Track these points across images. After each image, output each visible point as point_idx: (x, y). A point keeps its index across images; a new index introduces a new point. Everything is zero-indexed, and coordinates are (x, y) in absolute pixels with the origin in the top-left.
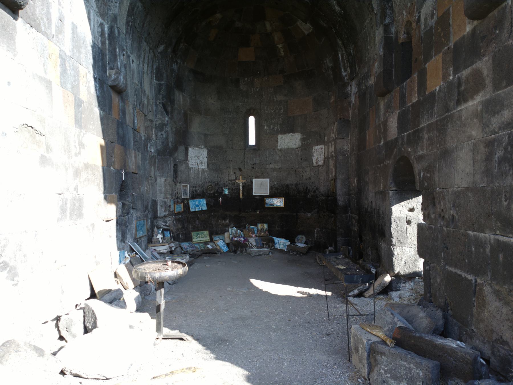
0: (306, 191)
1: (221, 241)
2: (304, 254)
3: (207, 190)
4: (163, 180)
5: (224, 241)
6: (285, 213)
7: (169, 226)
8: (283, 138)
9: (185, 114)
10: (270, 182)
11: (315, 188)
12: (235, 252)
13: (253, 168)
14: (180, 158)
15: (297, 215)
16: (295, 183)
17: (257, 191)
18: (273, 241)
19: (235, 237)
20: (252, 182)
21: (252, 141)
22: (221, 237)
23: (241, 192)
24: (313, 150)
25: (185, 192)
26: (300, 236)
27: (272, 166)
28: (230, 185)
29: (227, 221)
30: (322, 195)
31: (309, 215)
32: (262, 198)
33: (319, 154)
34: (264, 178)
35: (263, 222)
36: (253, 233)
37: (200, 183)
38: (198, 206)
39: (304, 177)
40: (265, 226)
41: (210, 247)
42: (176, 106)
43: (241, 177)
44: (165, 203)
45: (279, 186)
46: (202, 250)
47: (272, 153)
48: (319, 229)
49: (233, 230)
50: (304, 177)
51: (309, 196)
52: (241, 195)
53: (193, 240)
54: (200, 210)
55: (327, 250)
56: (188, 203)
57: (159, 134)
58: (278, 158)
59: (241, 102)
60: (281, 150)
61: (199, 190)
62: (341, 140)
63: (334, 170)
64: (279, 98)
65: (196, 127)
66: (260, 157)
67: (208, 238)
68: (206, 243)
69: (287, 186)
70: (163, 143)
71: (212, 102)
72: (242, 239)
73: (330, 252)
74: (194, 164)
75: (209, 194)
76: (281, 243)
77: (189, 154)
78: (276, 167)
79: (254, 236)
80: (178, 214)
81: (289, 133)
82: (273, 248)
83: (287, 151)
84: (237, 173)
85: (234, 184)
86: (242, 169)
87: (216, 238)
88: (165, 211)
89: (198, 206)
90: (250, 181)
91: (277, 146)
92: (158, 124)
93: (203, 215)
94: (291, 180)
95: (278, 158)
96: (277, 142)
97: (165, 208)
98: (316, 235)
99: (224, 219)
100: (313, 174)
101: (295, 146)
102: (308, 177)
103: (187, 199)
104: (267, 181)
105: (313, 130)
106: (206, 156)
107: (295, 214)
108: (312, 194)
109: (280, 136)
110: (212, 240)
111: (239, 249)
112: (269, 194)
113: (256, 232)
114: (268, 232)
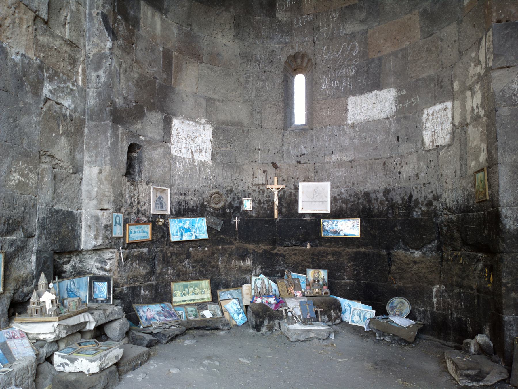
0: (410, 203)
1: (235, 301)
2: (407, 343)
3: (209, 202)
4: (95, 170)
5: (240, 302)
6: (363, 250)
7: (110, 270)
8: (359, 102)
9: (167, 56)
10: (332, 187)
11: (430, 196)
12: (257, 327)
13: (299, 162)
14: (150, 135)
15: (389, 254)
16: (383, 188)
17: (305, 207)
18: (338, 307)
19: (260, 295)
20: (296, 189)
21: (300, 117)
22: (235, 292)
23: (276, 208)
24: (425, 116)
25: (160, 203)
26: (397, 301)
27: (334, 158)
28: (256, 195)
29: (248, 263)
30: (449, 209)
31: (417, 254)
32: (317, 218)
33: (437, 122)
34: (320, 180)
35: (318, 266)
36: (298, 287)
37: (196, 187)
38: (188, 230)
39: (404, 176)
40: (323, 274)
41: (207, 314)
42: (142, 32)
43: (276, 179)
44: (97, 219)
45: (350, 196)
46: (188, 321)
47: (336, 133)
48: (443, 288)
49: (260, 281)
50: (404, 176)
51: (416, 214)
52: (276, 212)
53: (174, 299)
54: (193, 238)
55: (472, 342)
56: (166, 225)
57: (94, 75)
58: (347, 142)
59: (278, 43)
60: (353, 126)
61: (193, 201)
62: (502, 71)
63: (484, 146)
64: (350, 28)
65: (190, 81)
66: (312, 141)
67: (207, 296)
68: (201, 306)
69: (367, 194)
70: (99, 94)
71: (223, 41)
72: (272, 301)
73: (482, 350)
74: (184, 151)
75: (215, 209)
76: (357, 312)
77: (174, 131)
78: (344, 158)
79: (298, 294)
80: (138, 244)
81: (370, 91)
82: (338, 321)
83: (367, 127)
84: (269, 172)
85: (264, 192)
86: (279, 165)
87: (223, 294)
88: (96, 238)
89: (188, 230)
90: (293, 187)
91: (345, 119)
92: (91, 55)
93: (199, 249)
94: (375, 183)
95: (347, 142)
96: (346, 110)
97: (97, 230)
98: (435, 300)
99: (243, 257)
100: (423, 166)
101: (383, 116)
102: (412, 173)
103: (163, 216)
104: (325, 188)
105: (424, 75)
106: (210, 138)
107: (385, 252)
108: (424, 209)
109: (351, 100)
110: (215, 299)
111: (266, 323)
112: (329, 211)
113: (303, 286)
114: (329, 287)
